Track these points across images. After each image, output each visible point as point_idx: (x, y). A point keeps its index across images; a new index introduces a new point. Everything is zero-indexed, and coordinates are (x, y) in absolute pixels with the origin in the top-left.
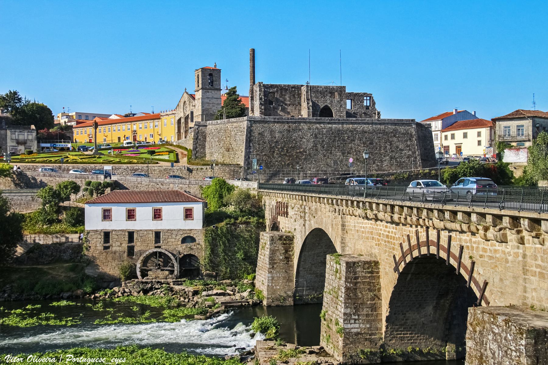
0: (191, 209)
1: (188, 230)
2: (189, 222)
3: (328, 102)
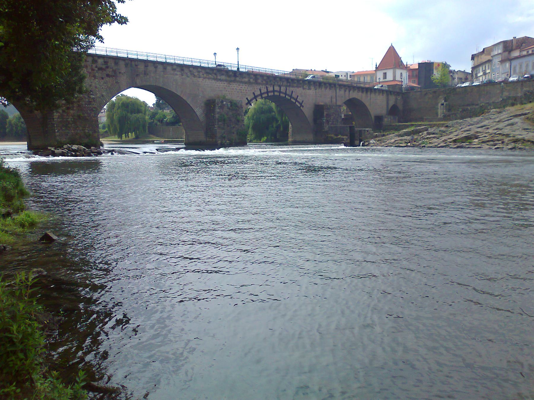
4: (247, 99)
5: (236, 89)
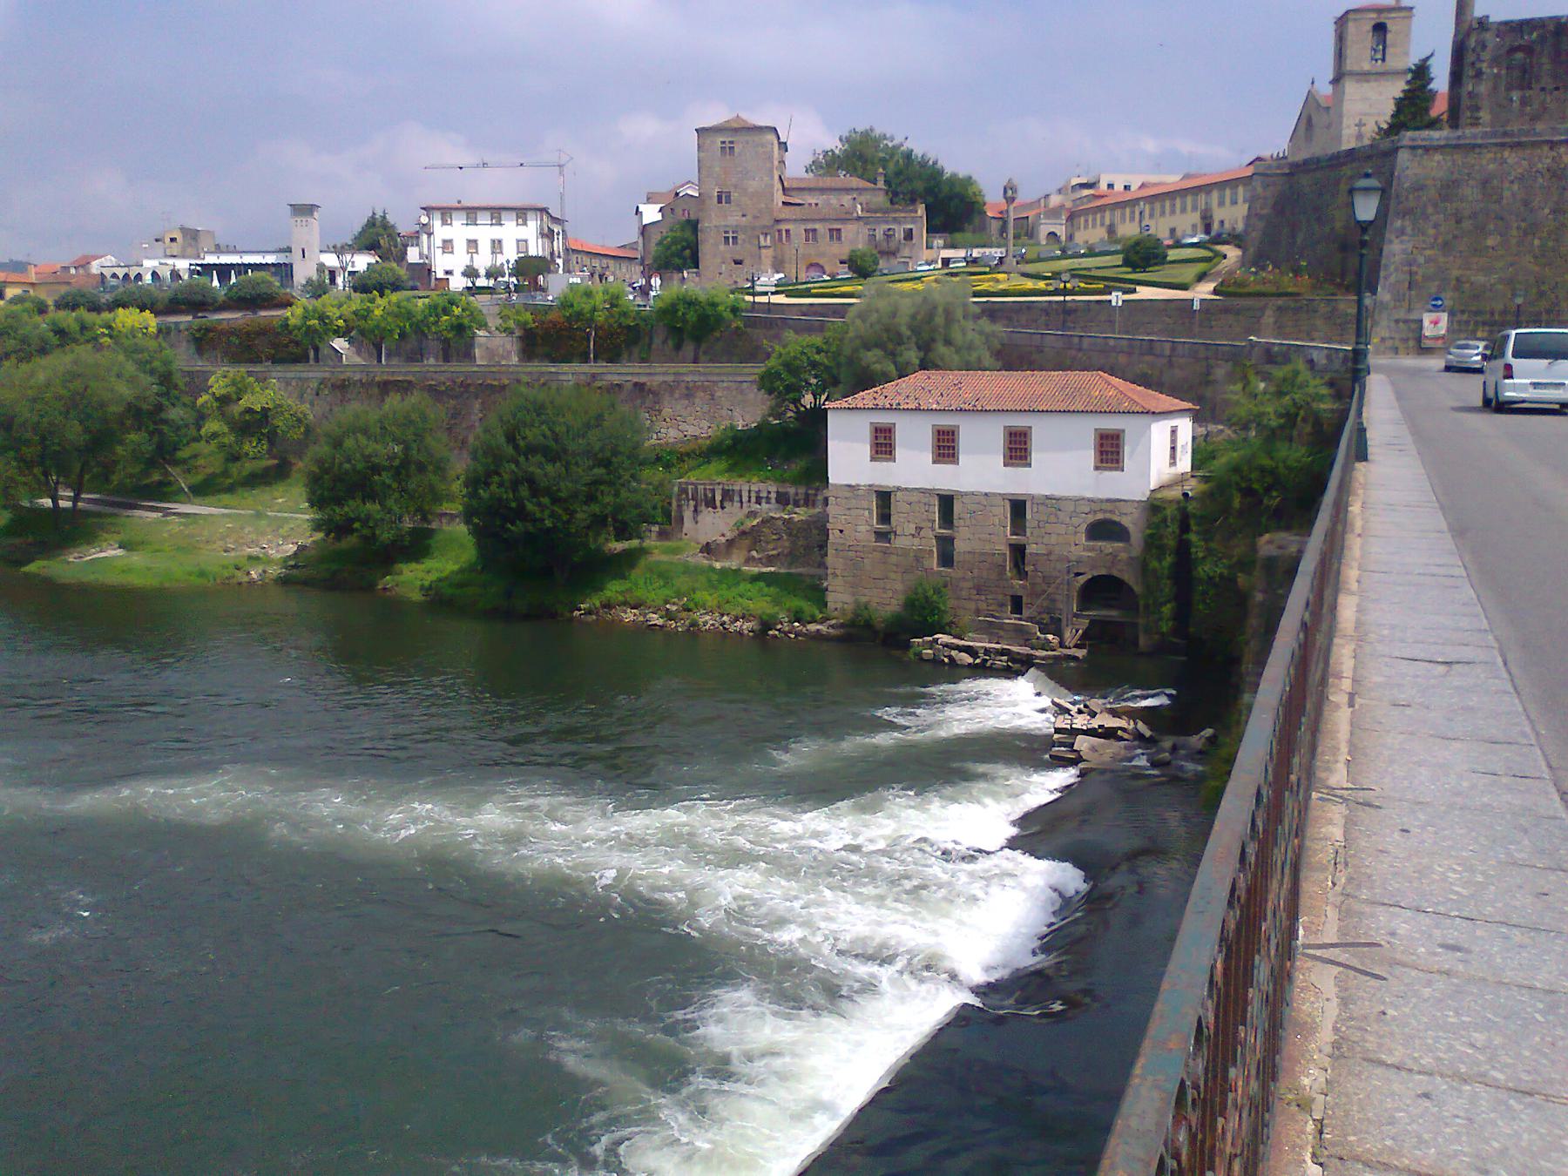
0: (1118, 437)
1: (1108, 501)
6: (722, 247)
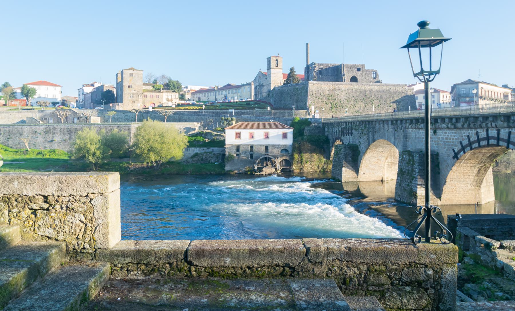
2: (285, 140)
3: (355, 73)
4: (454, 150)
5: (443, 138)
6: (129, 98)
